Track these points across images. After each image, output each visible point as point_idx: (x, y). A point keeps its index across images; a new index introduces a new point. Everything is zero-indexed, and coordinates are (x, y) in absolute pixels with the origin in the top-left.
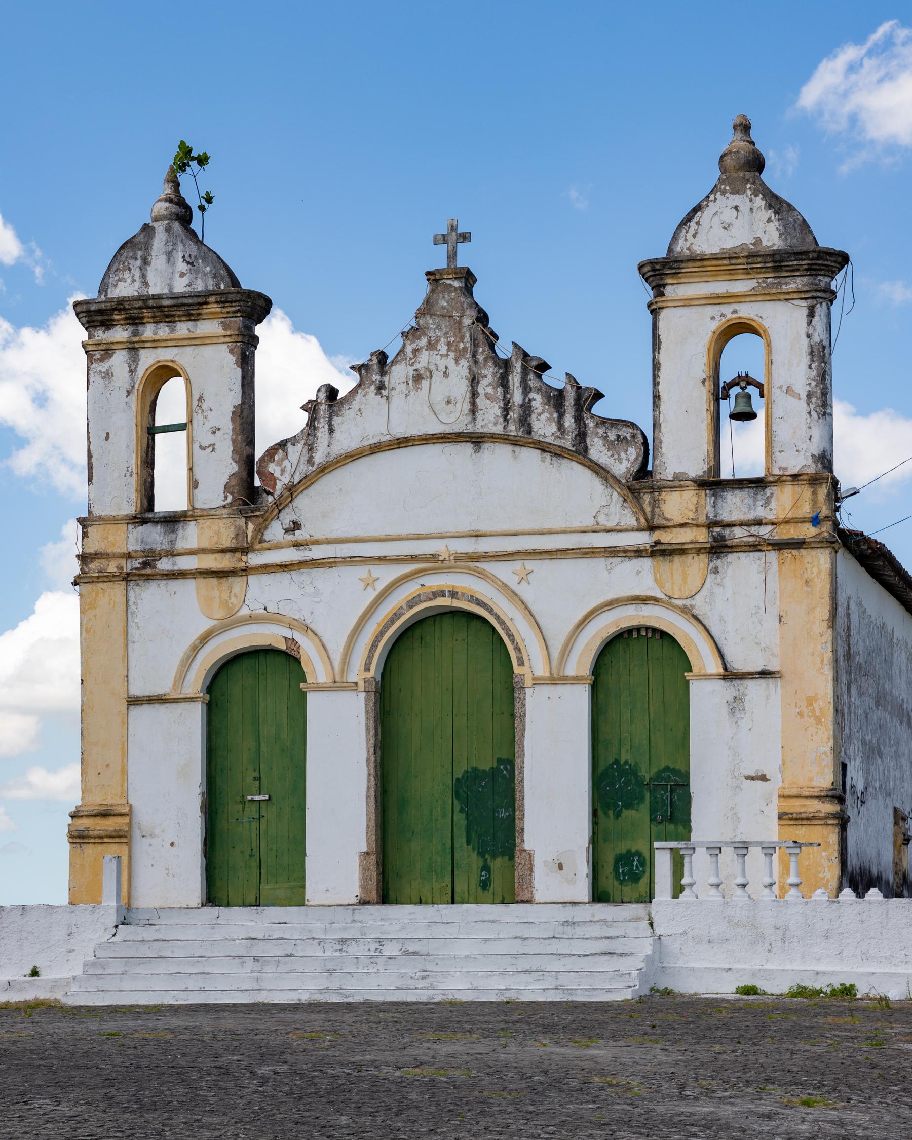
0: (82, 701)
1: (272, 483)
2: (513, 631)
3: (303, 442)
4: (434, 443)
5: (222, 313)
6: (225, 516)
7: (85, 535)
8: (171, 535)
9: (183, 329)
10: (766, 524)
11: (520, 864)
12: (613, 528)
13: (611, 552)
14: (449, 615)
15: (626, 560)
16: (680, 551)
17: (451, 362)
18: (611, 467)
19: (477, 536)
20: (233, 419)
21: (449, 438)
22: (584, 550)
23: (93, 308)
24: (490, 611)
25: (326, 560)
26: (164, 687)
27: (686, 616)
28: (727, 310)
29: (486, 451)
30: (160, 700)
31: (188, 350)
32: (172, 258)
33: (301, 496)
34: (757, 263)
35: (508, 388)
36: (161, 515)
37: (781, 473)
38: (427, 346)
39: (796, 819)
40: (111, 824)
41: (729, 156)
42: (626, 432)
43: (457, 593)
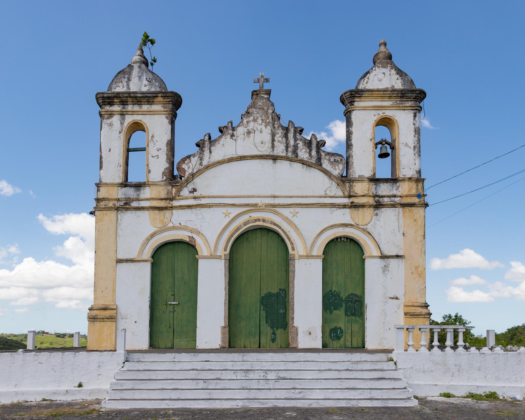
0: (95, 260)
1: (184, 172)
2: (290, 236)
3: (198, 156)
4: (256, 159)
5: (163, 101)
6: (162, 185)
7: (98, 191)
8: (138, 192)
9: (145, 107)
10: (398, 197)
11: (292, 332)
12: (333, 196)
13: (333, 205)
14: (260, 230)
15: (339, 209)
16: (363, 206)
17: (263, 127)
18: (332, 172)
19: (274, 197)
20: (167, 146)
21: (263, 157)
22: (322, 204)
23: (105, 95)
24: (280, 228)
25: (208, 204)
26: (133, 255)
27: (364, 232)
28: (380, 113)
29: (278, 163)
30: (132, 261)
31: (148, 116)
32: (141, 79)
33: (197, 178)
34: (394, 94)
35: (288, 138)
36: (134, 183)
37: (404, 177)
38: (253, 120)
39: (413, 315)
40: (108, 313)
41: (381, 53)
42: (338, 158)
43: (265, 220)
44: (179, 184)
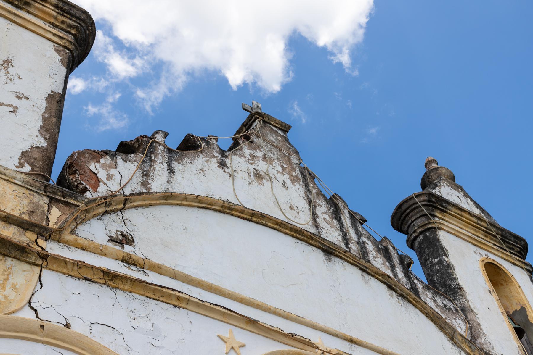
1: (93, 182)
44: (76, 203)
